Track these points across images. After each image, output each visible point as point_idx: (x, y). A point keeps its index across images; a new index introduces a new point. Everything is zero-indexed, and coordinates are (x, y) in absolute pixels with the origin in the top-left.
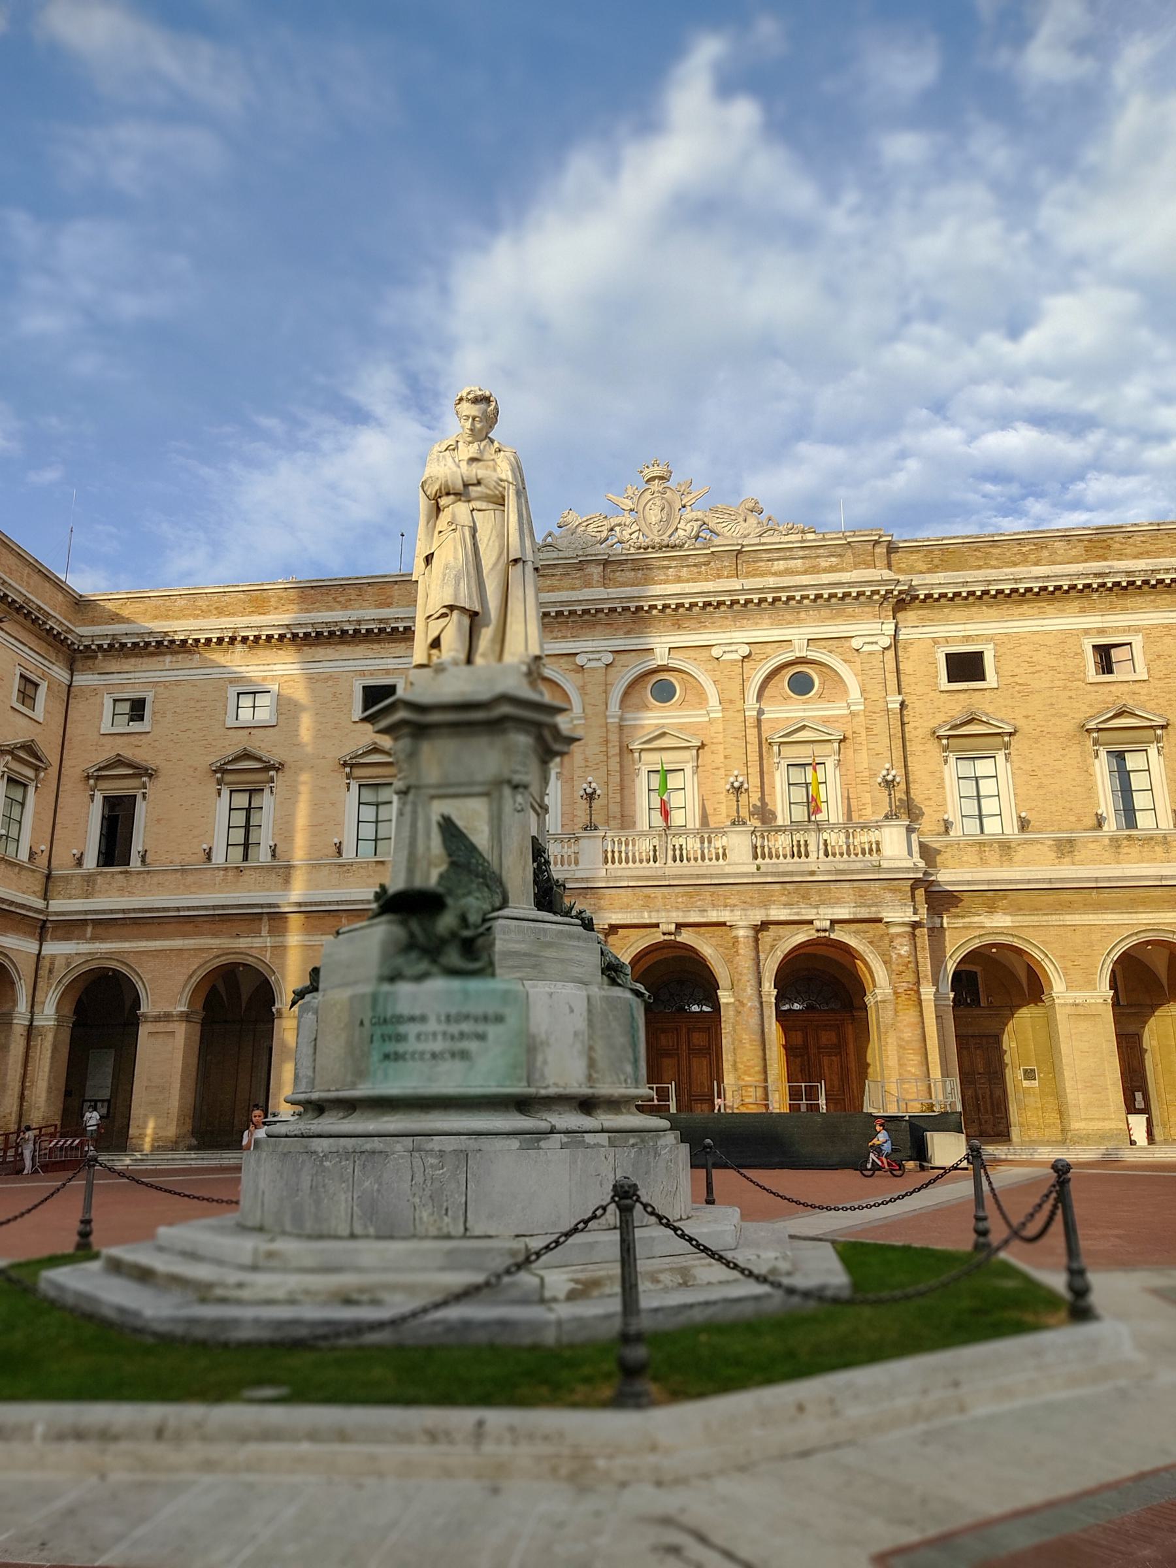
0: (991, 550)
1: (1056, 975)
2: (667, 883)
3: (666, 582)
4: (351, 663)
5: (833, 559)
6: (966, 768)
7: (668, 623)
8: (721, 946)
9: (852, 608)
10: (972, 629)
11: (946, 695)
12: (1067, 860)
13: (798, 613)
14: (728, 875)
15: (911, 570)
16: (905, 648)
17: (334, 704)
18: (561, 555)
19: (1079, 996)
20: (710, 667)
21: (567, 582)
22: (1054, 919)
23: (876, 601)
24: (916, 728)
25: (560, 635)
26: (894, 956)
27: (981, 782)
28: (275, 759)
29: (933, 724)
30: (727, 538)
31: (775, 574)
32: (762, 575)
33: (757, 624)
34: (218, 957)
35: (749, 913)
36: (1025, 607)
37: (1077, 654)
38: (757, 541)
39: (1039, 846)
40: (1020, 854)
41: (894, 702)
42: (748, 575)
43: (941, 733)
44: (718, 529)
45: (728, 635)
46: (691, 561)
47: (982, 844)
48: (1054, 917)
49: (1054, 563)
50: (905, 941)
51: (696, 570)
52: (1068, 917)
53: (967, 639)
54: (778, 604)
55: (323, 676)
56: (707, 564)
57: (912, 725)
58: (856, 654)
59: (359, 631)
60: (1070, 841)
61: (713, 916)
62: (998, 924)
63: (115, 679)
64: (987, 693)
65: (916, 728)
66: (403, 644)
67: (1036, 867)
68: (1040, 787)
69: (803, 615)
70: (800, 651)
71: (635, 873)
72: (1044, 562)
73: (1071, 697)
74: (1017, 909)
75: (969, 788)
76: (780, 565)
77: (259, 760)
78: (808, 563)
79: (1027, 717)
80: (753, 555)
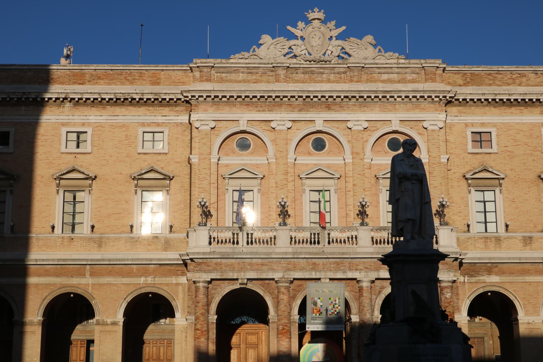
0: (496, 75)
1: (520, 308)
2: (326, 257)
3: (322, 82)
4: (136, 117)
5: (414, 75)
6: (479, 196)
7: (323, 106)
8: (352, 291)
9: (424, 104)
10: (486, 119)
11: (471, 155)
12: (528, 247)
13: (395, 105)
14: (359, 253)
15: (454, 84)
16: (450, 128)
17: (126, 142)
18: (262, 61)
19: (530, 319)
20: (346, 133)
21: (265, 78)
22: (520, 279)
23: (436, 102)
24: (455, 173)
25: (261, 109)
26: (443, 298)
27: (486, 203)
28: (92, 175)
29: (464, 171)
30: (355, 58)
31: (383, 81)
32: (376, 81)
33: (372, 110)
34: (60, 288)
35: (369, 274)
36: (513, 109)
37: (538, 136)
38: (372, 61)
39: (515, 240)
40: (504, 244)
41: (444, 158)
42: (368, 81)
43: (468, 176)
44: (350, 52)
45: (356, 115)
46: (336, 70)
47: (486, 238)
48: (521, 278)
49: (528, 85)
50: (449, 290)
51: (338, 76)
52: (527, 278)
53: (483, 124)
54: (383, 99)
55: (119, 125)
56: (345, 73)
57: (453, 171)
58: (425, 130)
59: (142, 99)
60: (530, 238)
61: (350, 275)
62: (492, 282)
64: (492, 155)
65: (455, 173)
66: (167, 108)
67: (512, 252)
68: (517, 208)
69: (397, 106)
70: (395, 127)
71: (308, 250)
72: (523, 84)
73: (534, 160)
74: (501, 273)
75: (481, 207)
76: (385, 77)
77: (83, 173)
78: (401, 76)
79: (512, 170)
80: (370, 69)
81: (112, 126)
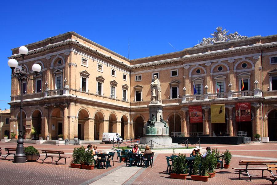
63: (136, 73)
81: (164, 71)
